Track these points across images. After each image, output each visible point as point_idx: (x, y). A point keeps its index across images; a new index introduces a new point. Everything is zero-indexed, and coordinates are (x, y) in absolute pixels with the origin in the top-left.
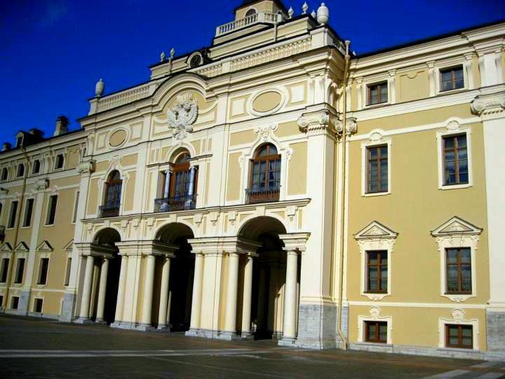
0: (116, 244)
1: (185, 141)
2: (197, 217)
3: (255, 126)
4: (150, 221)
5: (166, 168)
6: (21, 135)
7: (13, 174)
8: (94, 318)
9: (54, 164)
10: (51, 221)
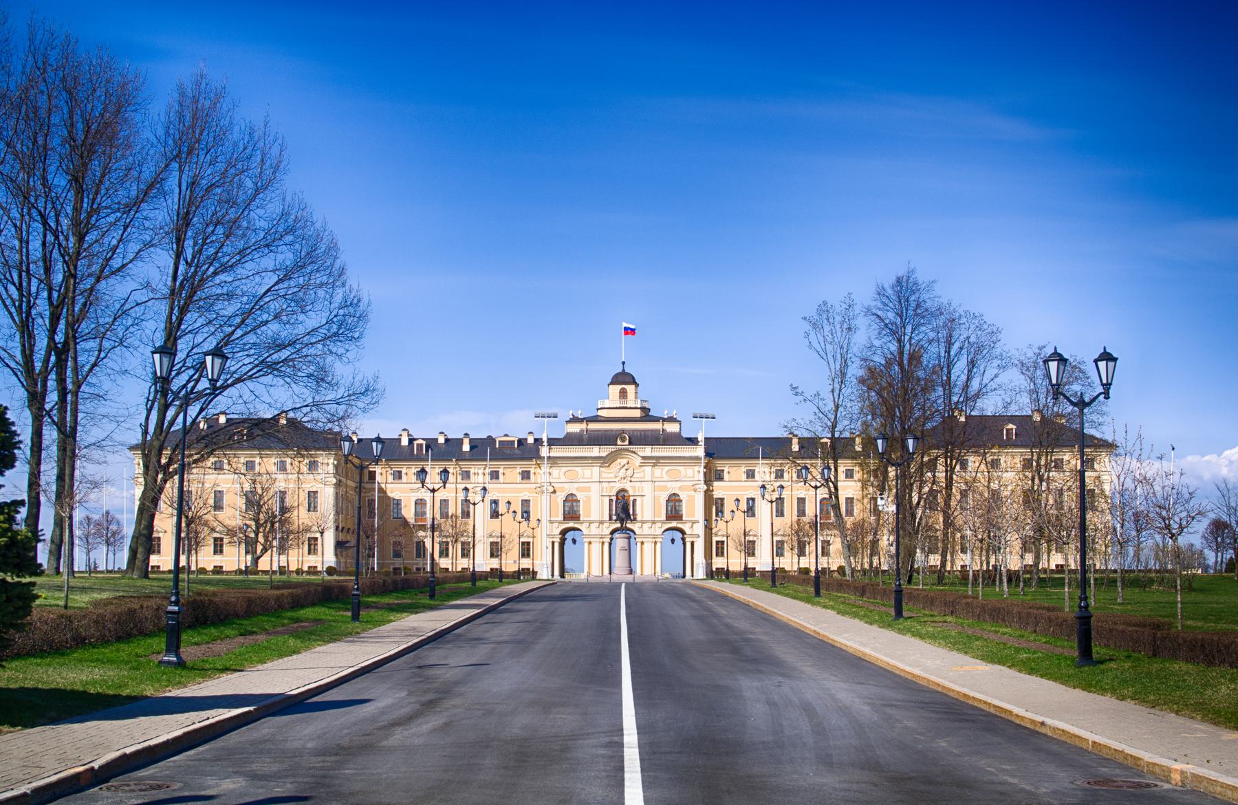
2: (638, 525)
3: (669, 484)
4: (606, 525)
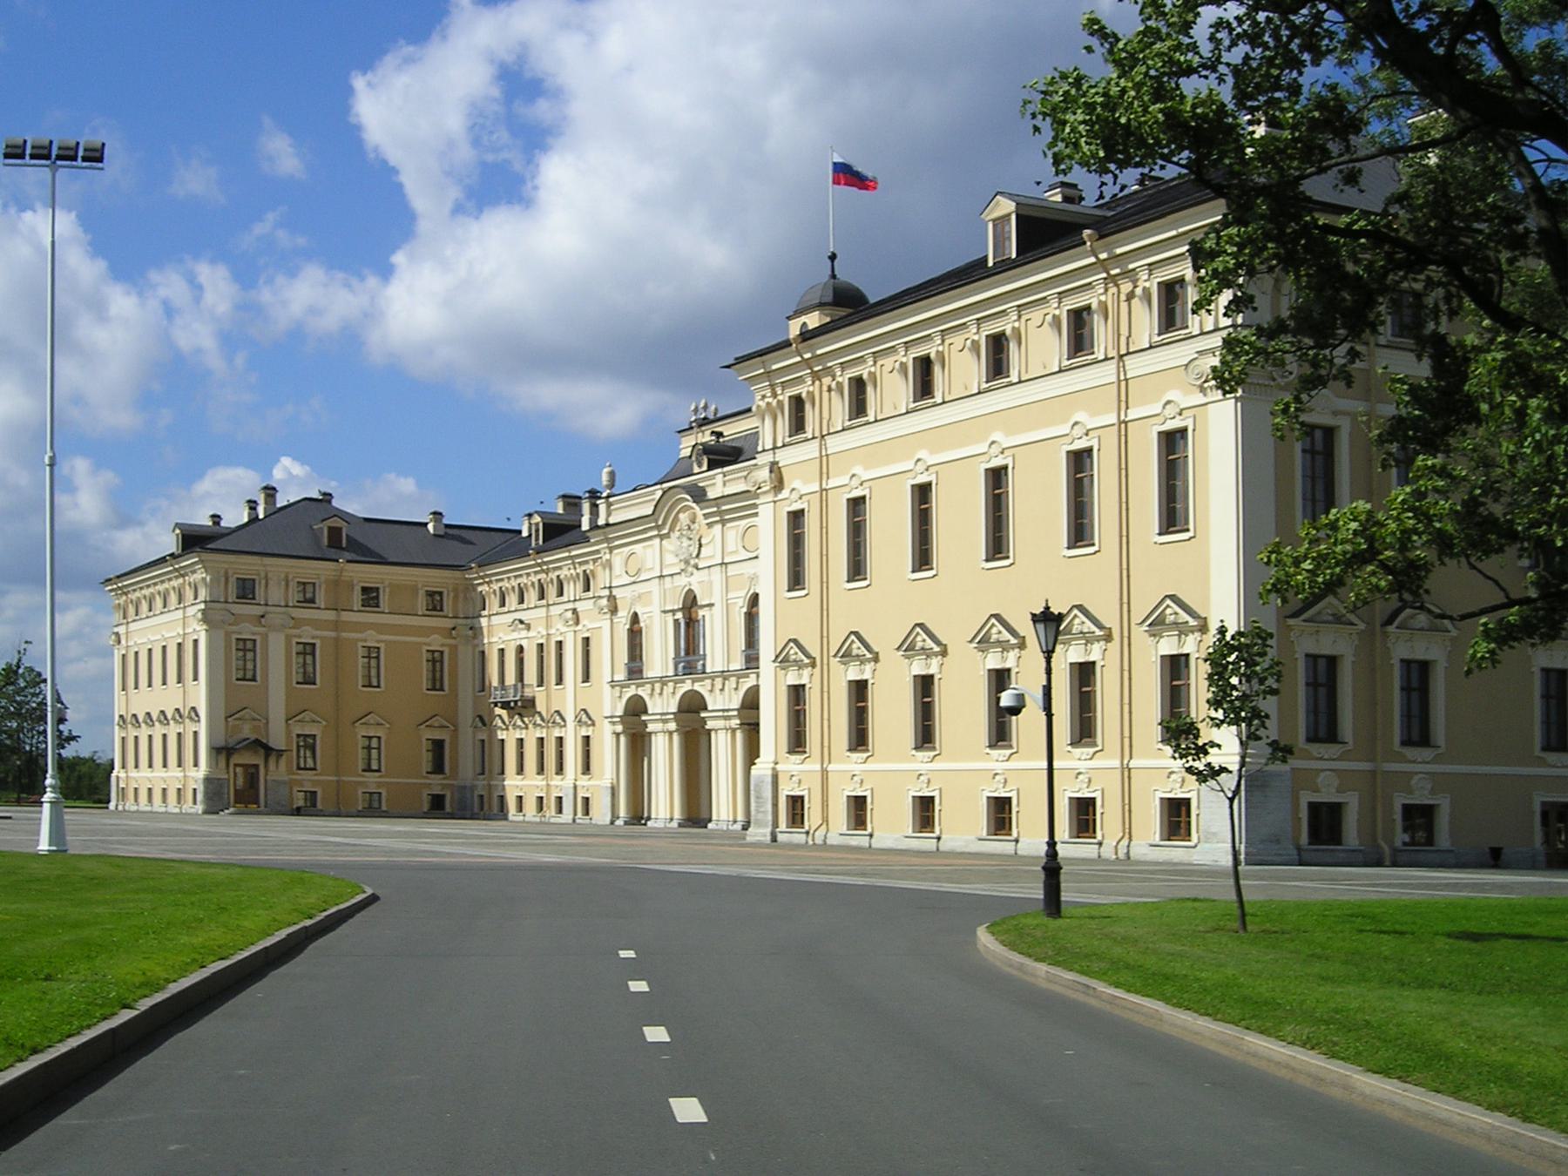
0: (644, 718)
1: (692, 579)
5: (679, 615)
6: (537, 519)
7: (532, 596)
8: (638, 816)
9: (580, 585)
10: (586, 678)
